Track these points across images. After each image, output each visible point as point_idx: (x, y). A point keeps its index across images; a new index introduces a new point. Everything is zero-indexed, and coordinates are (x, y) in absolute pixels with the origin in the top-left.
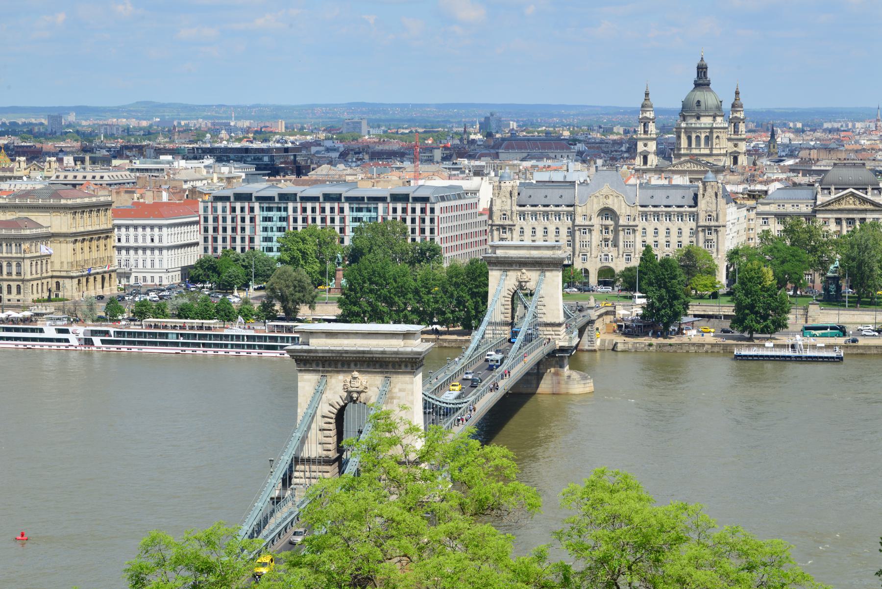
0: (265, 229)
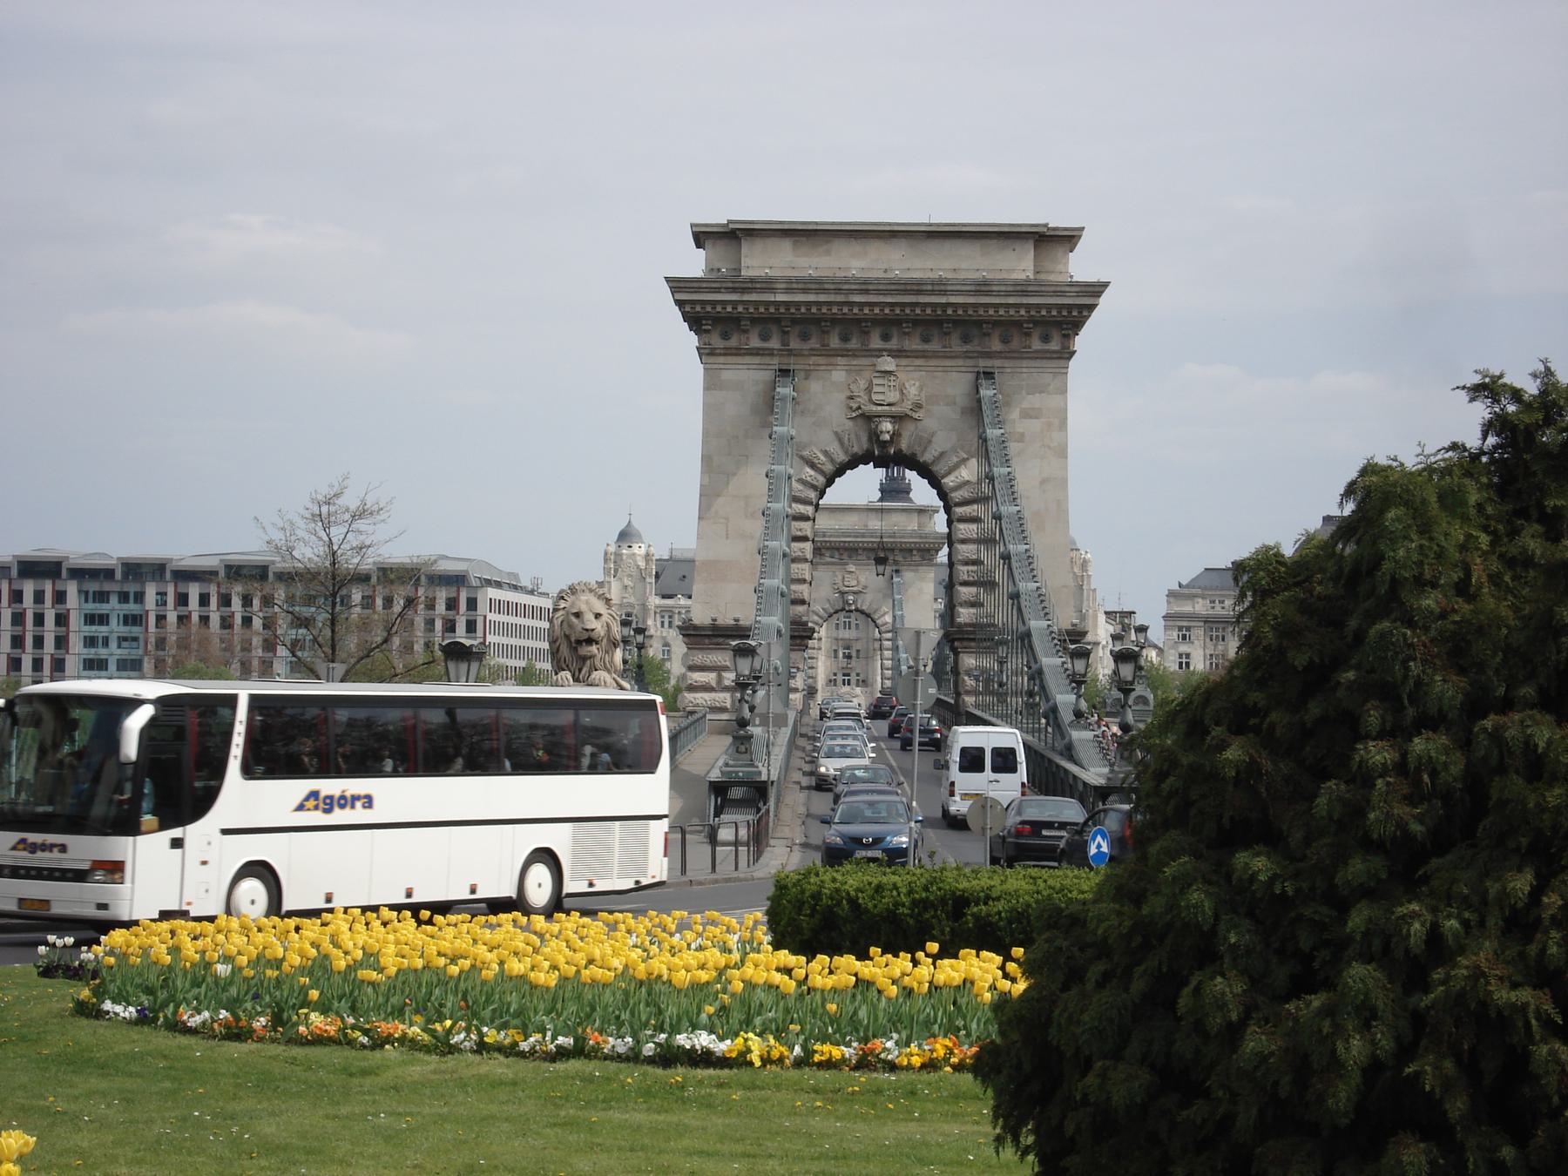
0: (90, 642)
